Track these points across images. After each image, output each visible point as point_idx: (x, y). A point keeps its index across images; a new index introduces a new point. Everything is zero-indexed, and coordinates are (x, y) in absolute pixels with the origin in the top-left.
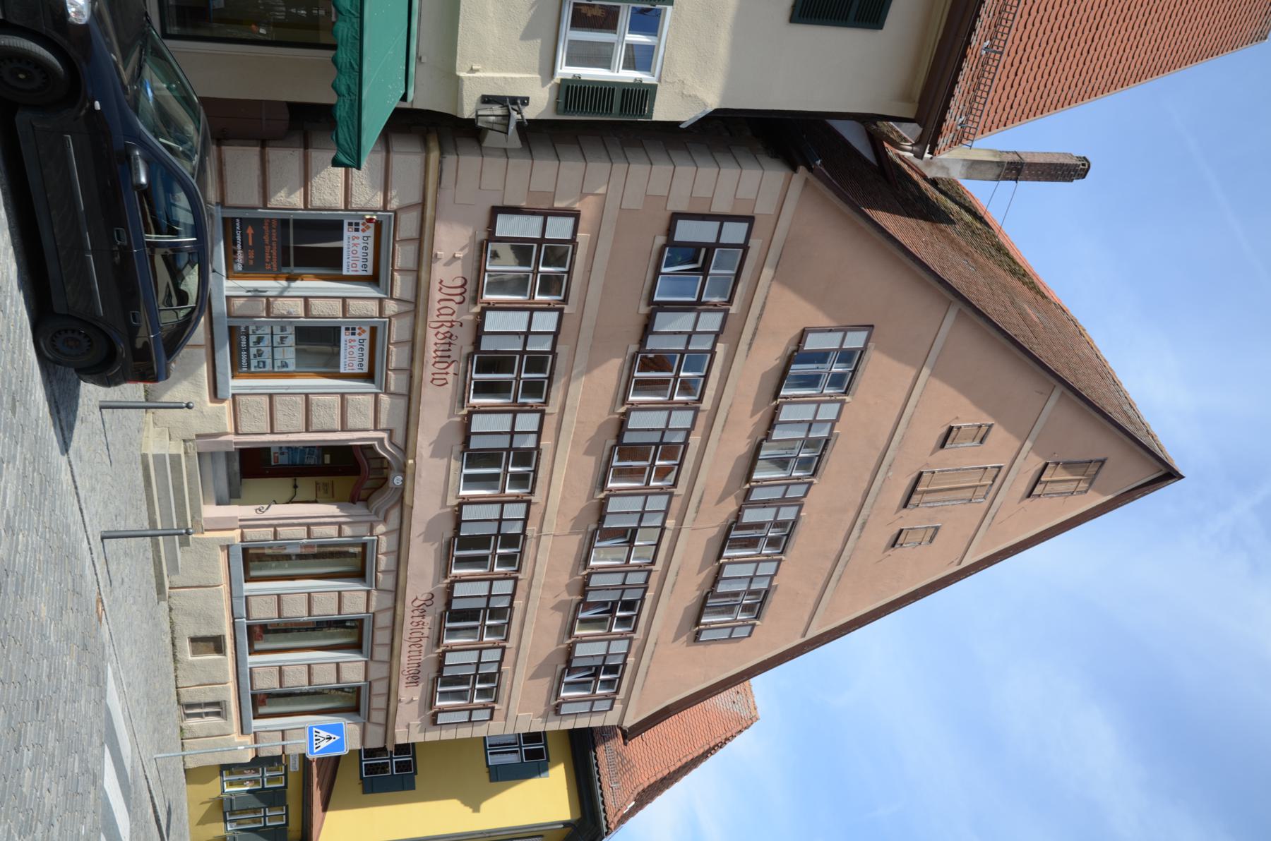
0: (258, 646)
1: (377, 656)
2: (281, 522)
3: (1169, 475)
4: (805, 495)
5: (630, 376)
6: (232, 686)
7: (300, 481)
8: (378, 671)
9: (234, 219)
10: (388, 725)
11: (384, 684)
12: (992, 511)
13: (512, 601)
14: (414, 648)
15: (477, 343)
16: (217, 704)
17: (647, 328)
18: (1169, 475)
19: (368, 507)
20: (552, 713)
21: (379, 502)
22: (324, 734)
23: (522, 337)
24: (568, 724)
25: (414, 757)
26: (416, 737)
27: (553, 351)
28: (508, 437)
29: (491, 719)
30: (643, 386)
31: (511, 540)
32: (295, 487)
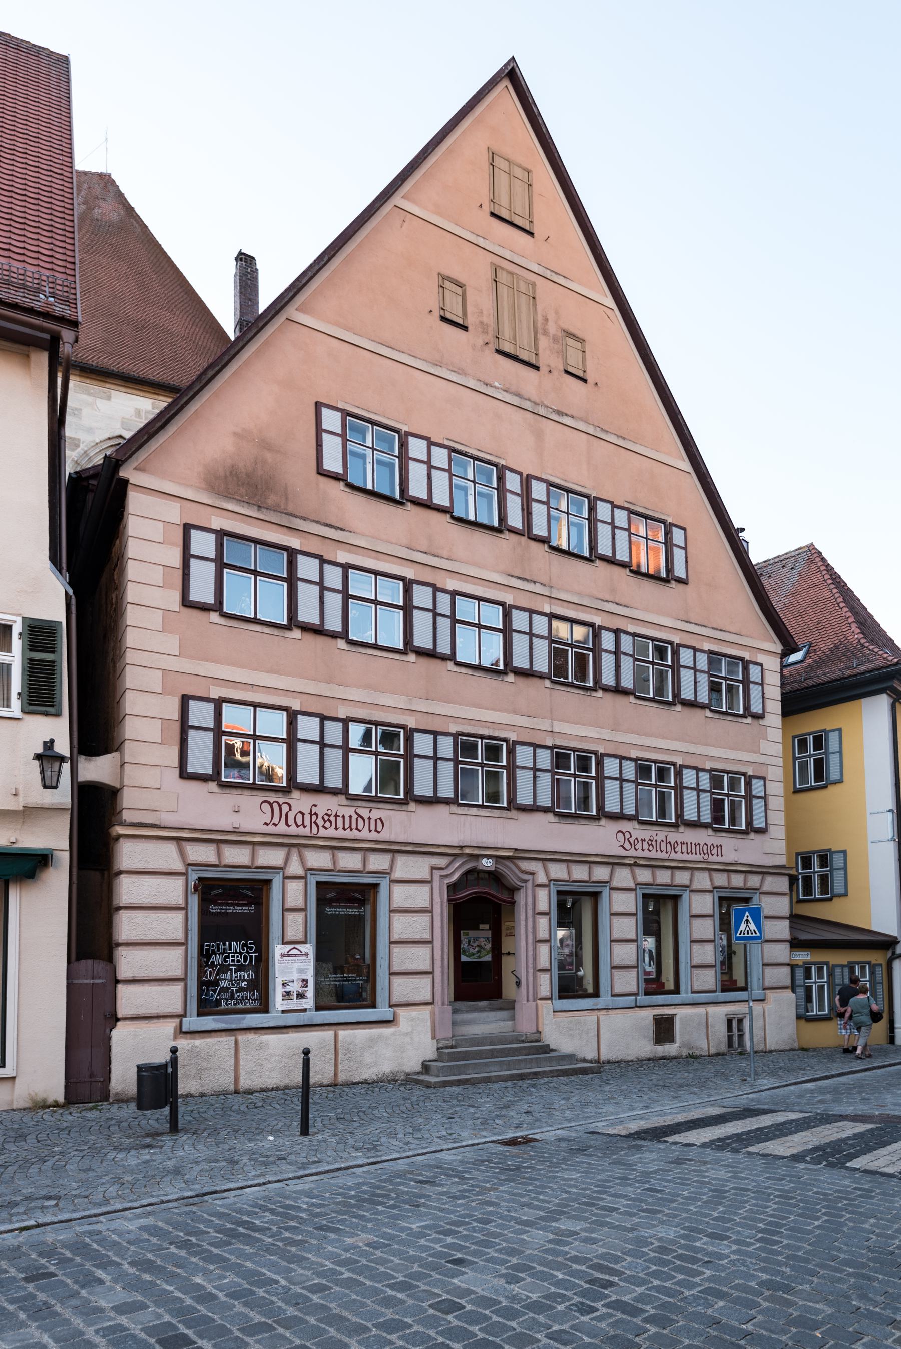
0: (741, 983)
1: (686, 882)
2: (531, 965)
3: (510, 73)
4: (520, 474)
5: (571, 685)
6: (711, 1009)
7: (504, 950)
8: (703, 880)
9: (645, 980)
10: (763, 871)
11: (716, 875)
12: (548, 274)
13: (704, 770)
14: (678, 849)
15: (705, 826)
16: (730, 1022)
17: (692, 704)
18: (510, 73)
19: (518, 889)
20: (761, 722)
21: (513, 879)
22: (743, 926)
23: (538, 774)
24: (775, 707)
25: (814, 852)
26: (781, 846)
27: (635, 760)
28: (625, 784)
29: (764, 778)
30: (581, 672)
31: (717, 782)
32: (509, 954)
